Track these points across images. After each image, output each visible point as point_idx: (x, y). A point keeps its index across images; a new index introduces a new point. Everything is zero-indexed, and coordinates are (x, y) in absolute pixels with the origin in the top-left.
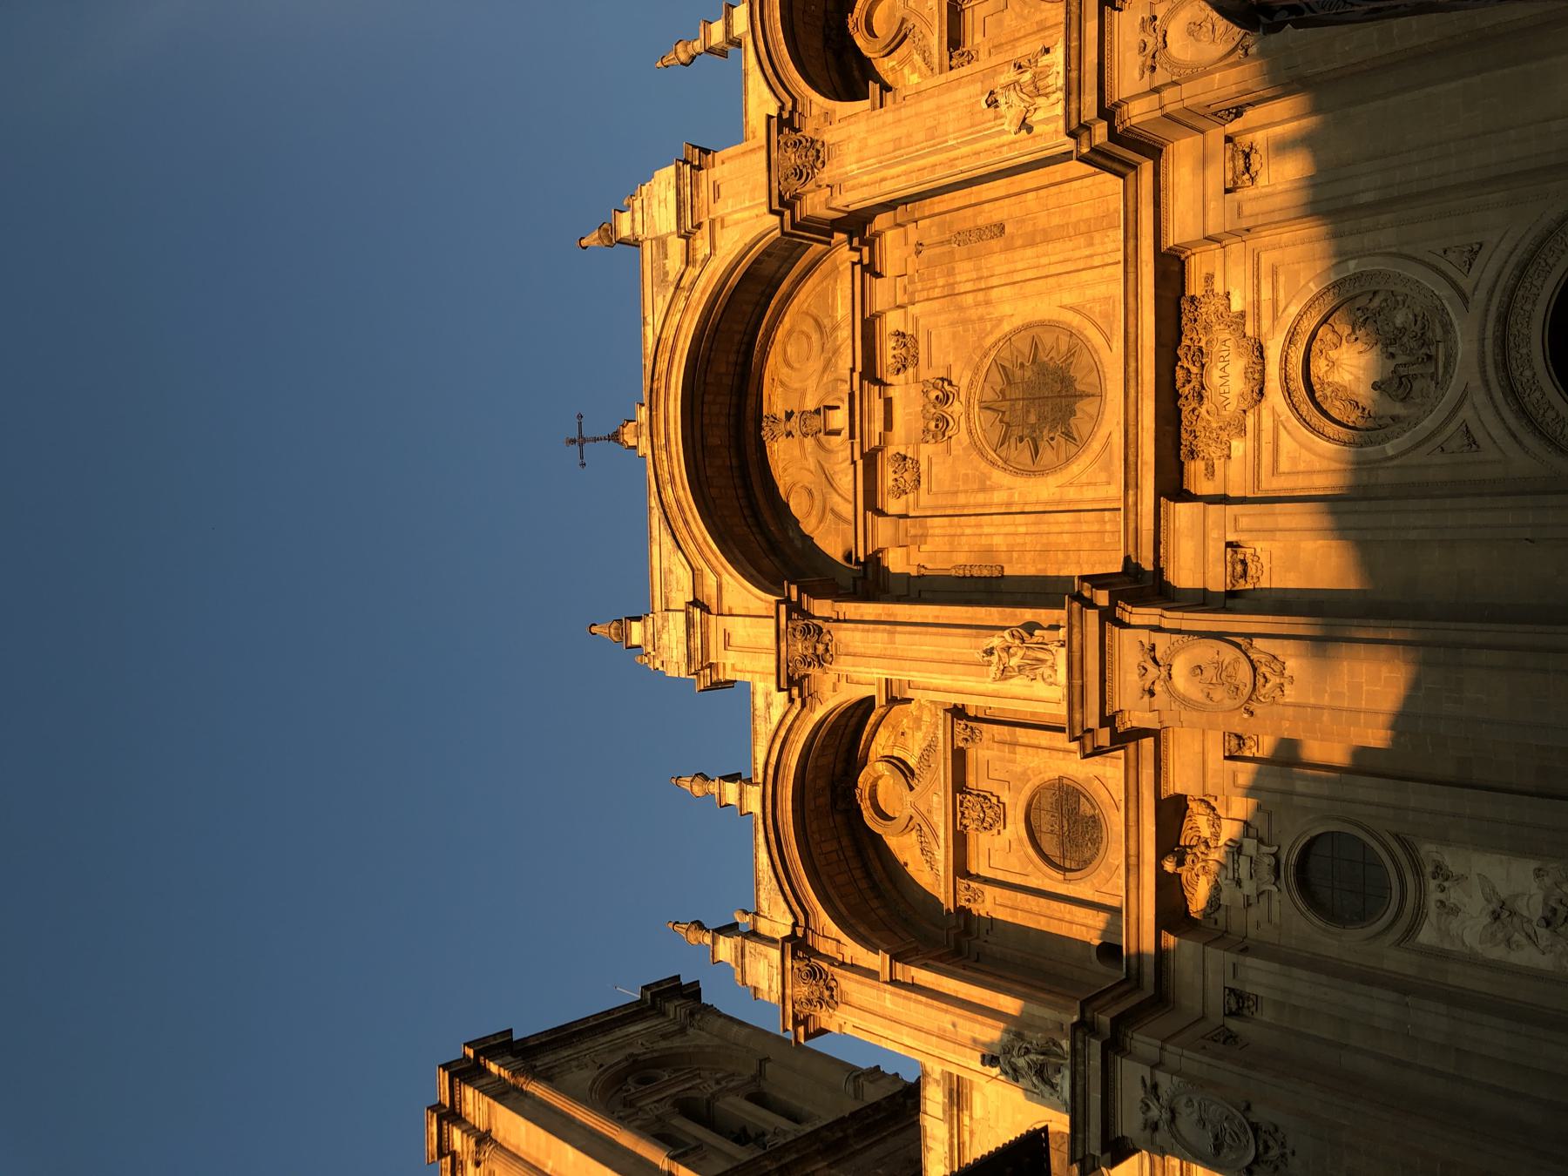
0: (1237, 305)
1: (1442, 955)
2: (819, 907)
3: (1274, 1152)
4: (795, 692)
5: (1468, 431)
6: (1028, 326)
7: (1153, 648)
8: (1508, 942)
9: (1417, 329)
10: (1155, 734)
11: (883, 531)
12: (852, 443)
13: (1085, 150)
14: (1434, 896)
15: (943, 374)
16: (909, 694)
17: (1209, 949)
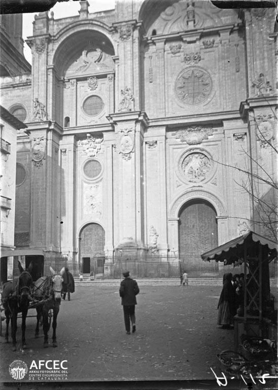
0: (209, 137)
1: (82, 188)
2: (60, 43)
3: (38, 165)
4: (112, 28)
5: (180, 185)
6: (212, 81)
7: (131, 131)
8: (87, 198)
9: (202, 174)
10: (113, 130)
11: (160, 45)
12: (183, 32)
13: (243, 104)
14: (93, 185)
15: (202, 58)
16: (116, 66)
17: (73, 145)
